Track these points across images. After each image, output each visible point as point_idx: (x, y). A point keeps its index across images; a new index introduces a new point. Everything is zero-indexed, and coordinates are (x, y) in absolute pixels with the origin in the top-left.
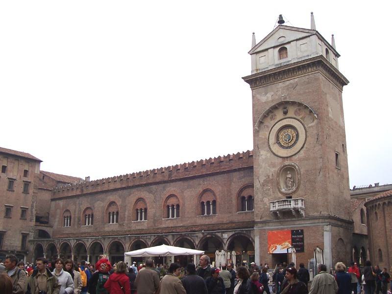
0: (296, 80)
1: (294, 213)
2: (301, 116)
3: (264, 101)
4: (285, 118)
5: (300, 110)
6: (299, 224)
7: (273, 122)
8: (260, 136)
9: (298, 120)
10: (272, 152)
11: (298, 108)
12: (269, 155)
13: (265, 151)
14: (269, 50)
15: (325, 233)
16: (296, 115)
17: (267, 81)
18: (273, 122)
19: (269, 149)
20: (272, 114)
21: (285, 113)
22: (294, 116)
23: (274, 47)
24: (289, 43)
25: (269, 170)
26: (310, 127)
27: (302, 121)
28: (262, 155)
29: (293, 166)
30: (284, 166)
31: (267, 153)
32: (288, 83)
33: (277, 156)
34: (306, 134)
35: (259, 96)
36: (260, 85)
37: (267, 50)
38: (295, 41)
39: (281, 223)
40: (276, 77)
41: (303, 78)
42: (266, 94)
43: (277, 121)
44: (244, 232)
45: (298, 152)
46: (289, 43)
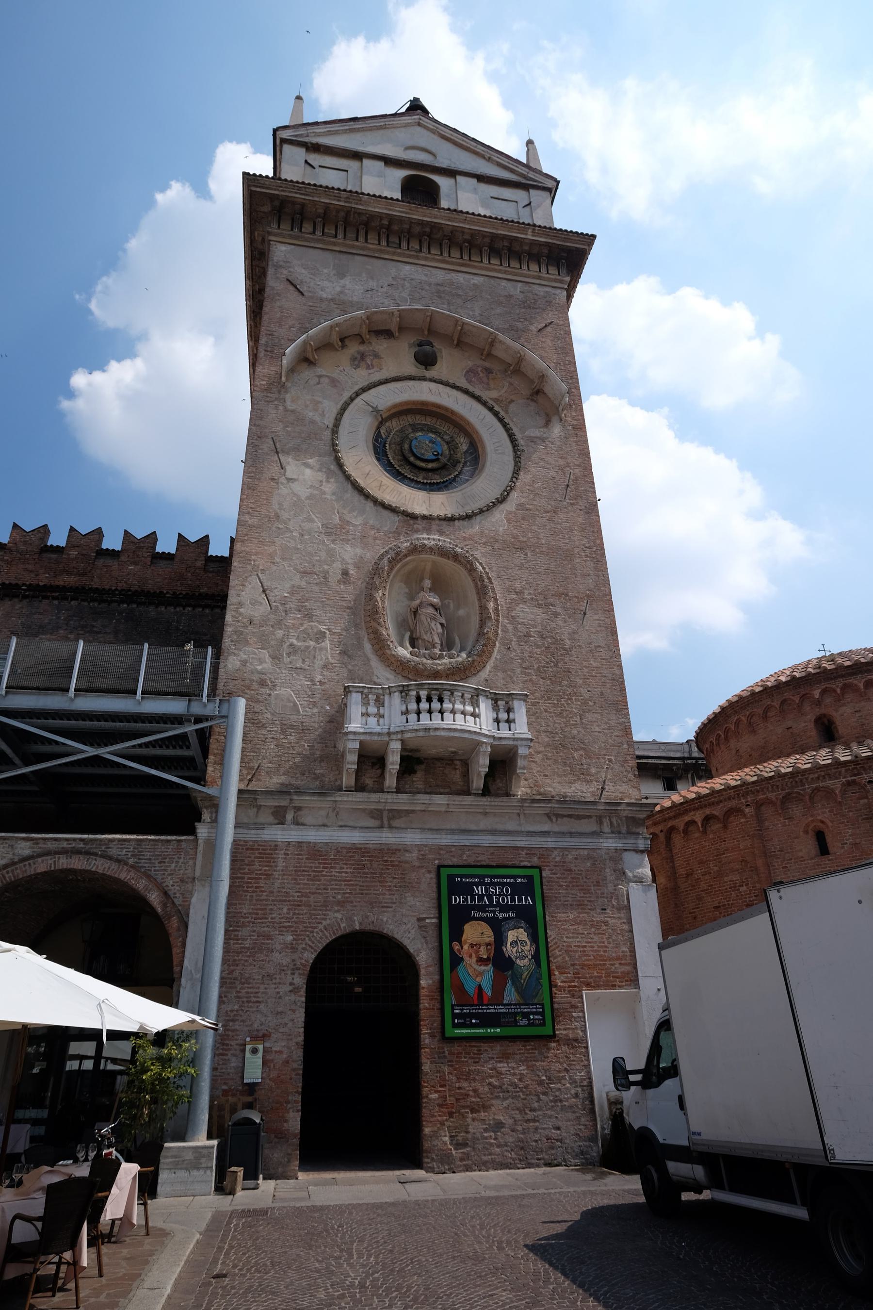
0: (477, 280)
1: (482, 764)
2: (494, 394)
3: (325, 296)
4: (423, 379)
5: (488, 371)
6: (493, 832)
7: (362, 376)
8: (290, 405)
9: (484, 404)
10: (348, 477)
11: (480, 362)
12: (329, 488)
13: (307, 465)
14: (365, 161)
15: (635, 890)
16: (470, 382)
18: (362, 376)
19: (333, 467)
20: (362, 348)
22: (463, 383)
23: (389, 161)
24: (451, 173)
25: (331, 553)
27: (502, 413)
28: (290, 480)
29: (455, 557)
30: (415, 549)
31: (321, 476)
32: (440, 276)
33: (376, 502)
35: (303, 271)
36: (318, 241)
37: (357, 156)
39: (385, 818)
40: (394, 239)
41: (504, 283)
43: (377, 377)
44: (114, 851)
45: (481, 511)
46: (451, 173)
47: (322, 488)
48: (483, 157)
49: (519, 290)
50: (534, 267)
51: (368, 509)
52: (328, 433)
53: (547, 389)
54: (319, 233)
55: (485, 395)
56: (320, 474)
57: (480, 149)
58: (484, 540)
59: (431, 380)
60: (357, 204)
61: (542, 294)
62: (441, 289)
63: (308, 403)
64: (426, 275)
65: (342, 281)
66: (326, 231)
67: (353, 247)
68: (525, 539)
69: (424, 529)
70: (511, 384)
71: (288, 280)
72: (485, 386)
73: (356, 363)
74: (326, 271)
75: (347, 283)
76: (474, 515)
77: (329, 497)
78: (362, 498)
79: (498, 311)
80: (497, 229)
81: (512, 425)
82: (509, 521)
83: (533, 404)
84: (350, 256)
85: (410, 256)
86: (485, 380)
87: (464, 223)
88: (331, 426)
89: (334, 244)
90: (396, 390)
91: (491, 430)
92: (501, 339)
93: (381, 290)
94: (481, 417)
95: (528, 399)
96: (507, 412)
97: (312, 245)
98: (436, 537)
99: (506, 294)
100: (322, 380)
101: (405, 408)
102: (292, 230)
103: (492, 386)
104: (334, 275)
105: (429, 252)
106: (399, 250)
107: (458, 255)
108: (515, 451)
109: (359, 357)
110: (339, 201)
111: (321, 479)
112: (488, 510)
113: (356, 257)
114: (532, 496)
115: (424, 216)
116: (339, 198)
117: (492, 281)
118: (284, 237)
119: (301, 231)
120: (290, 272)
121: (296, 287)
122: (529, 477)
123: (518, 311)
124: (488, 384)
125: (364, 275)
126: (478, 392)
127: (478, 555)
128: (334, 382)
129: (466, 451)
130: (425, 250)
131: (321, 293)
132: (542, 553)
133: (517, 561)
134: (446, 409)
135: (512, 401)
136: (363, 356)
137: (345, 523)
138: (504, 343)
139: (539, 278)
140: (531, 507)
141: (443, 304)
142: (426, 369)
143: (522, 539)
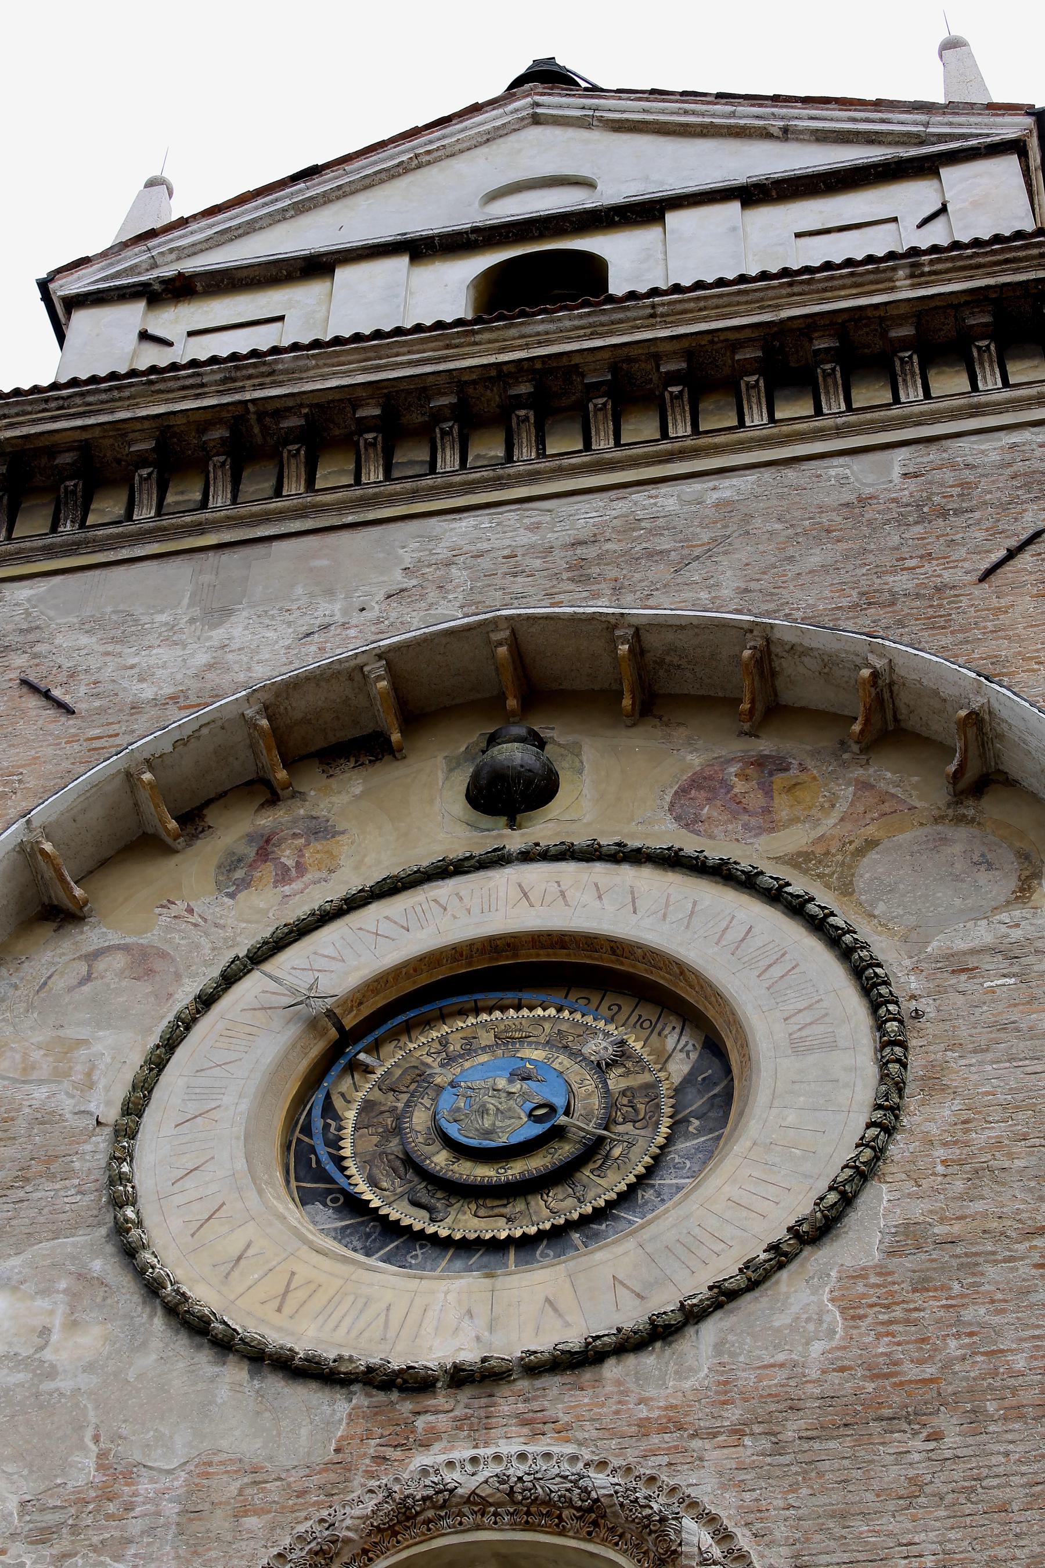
0: (728, 488)
3: (148, 692)
4: (497, 859)
5: (767, 767)
9: (747, 882)
10: (152, 1288)
14: (343, 274)
16: (690, 823)
17: (250, 488)
19: (104, 1264)
20: (266, 820)
21: (508, 796)
22: (664, 833)
26: (961, 965)
27: (824, 898)
31: (50, 1310)
32: (585, 515)
34: (892, 1047)
35: (84, 640)
38: (734, 207)
41: (836, 468)
42: (217, 613)
45: (724, 1297)
46: (647, 212)
47: (48, 1355)
48: (765, 134)
49: (897, 471)
50: (950, 383)
51: (223, 1393)
52: (101, 1143)
53: (1013, 766)
54: (145, 513)
55: (745, 854)
56: (42, 1303)
57: (746, 115)
58: (733, 1414)
59: (527, 857)
60: (262, 386)
61: (994, 457)
62: (591, 552)
63: (37, 1055)
64: (535, 527)
65: (218, 634)
66: (170, 499)
67: (265, 518)
68: (930, 1371)
69: (459, 1423)
70: (864, 786)
71: (24, 682)
72: (753, 822)
73: (239, 874)
74: (163, 618)
75: (237, 632)
76: (693, 1315)
77: (65, 1384)
78: (204, 1359)
79: (815, 558)
80: (778, 307)
81: (865, 931)
82: (851, 1311)
83: (962, 833)
84: (259, 550)
85: (470, 487)
86: (756, 800)
87: (651, 327)
88: (112, 1114)
89: (199, 528)
90: (385, 928)
91: (777, 971)
92: (789, 638)
93: (357, 618)
94: (735, 934)
95: (937, 820)
96: (846, 889)
97: (125, 554)
98: (509, 1448)
99: (848, 497)
100: (101, 965)
101: (424, 980)
102: (54, 529)
103: (784, 814)
104: (192, 621)
105: (542, 454)
106: (428, 482)
107: (649, 429)
108: (880, 1026)
109: (251, 852)
110: (198, 396)
111: (38, 1322)
112: (753, 1285)
113: (276, 545)
114: (959, 1186)
115: (502, 350)
116: (199, 389)
117: (790, 474)
118: (28, 560)
119: (82, 525)
120: (35, 656)
121: (47, 695)
122: (947, 1110)
123: (896, 540)
124: (767, 811)
125: (299, 590)
126: (714, 853)
127: (701, 1484)
128: (144, 962)
129: (688, 1080)
130: (526, 452)
131: (136, 687)
132: (1016, 1412)
133: (893, 1475)
134: (590, 942)
135: (871, 844)
136: (265, 847)
137: (117, 1474)
138: (807, 652)
139: (977, 410)
140: (957, 1228)
141: (596, 595)
142: (512, 824)
143: (911, 1371)
